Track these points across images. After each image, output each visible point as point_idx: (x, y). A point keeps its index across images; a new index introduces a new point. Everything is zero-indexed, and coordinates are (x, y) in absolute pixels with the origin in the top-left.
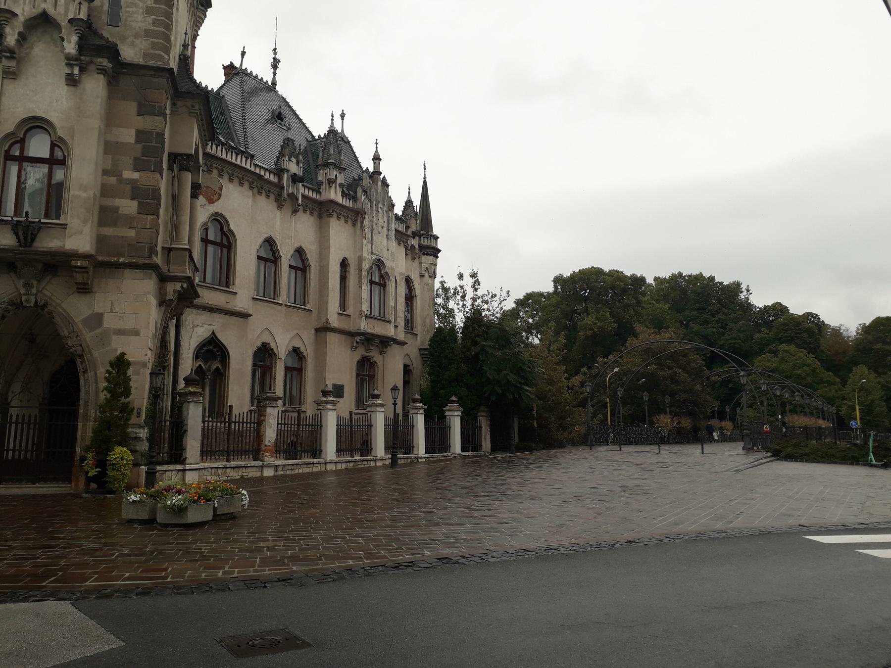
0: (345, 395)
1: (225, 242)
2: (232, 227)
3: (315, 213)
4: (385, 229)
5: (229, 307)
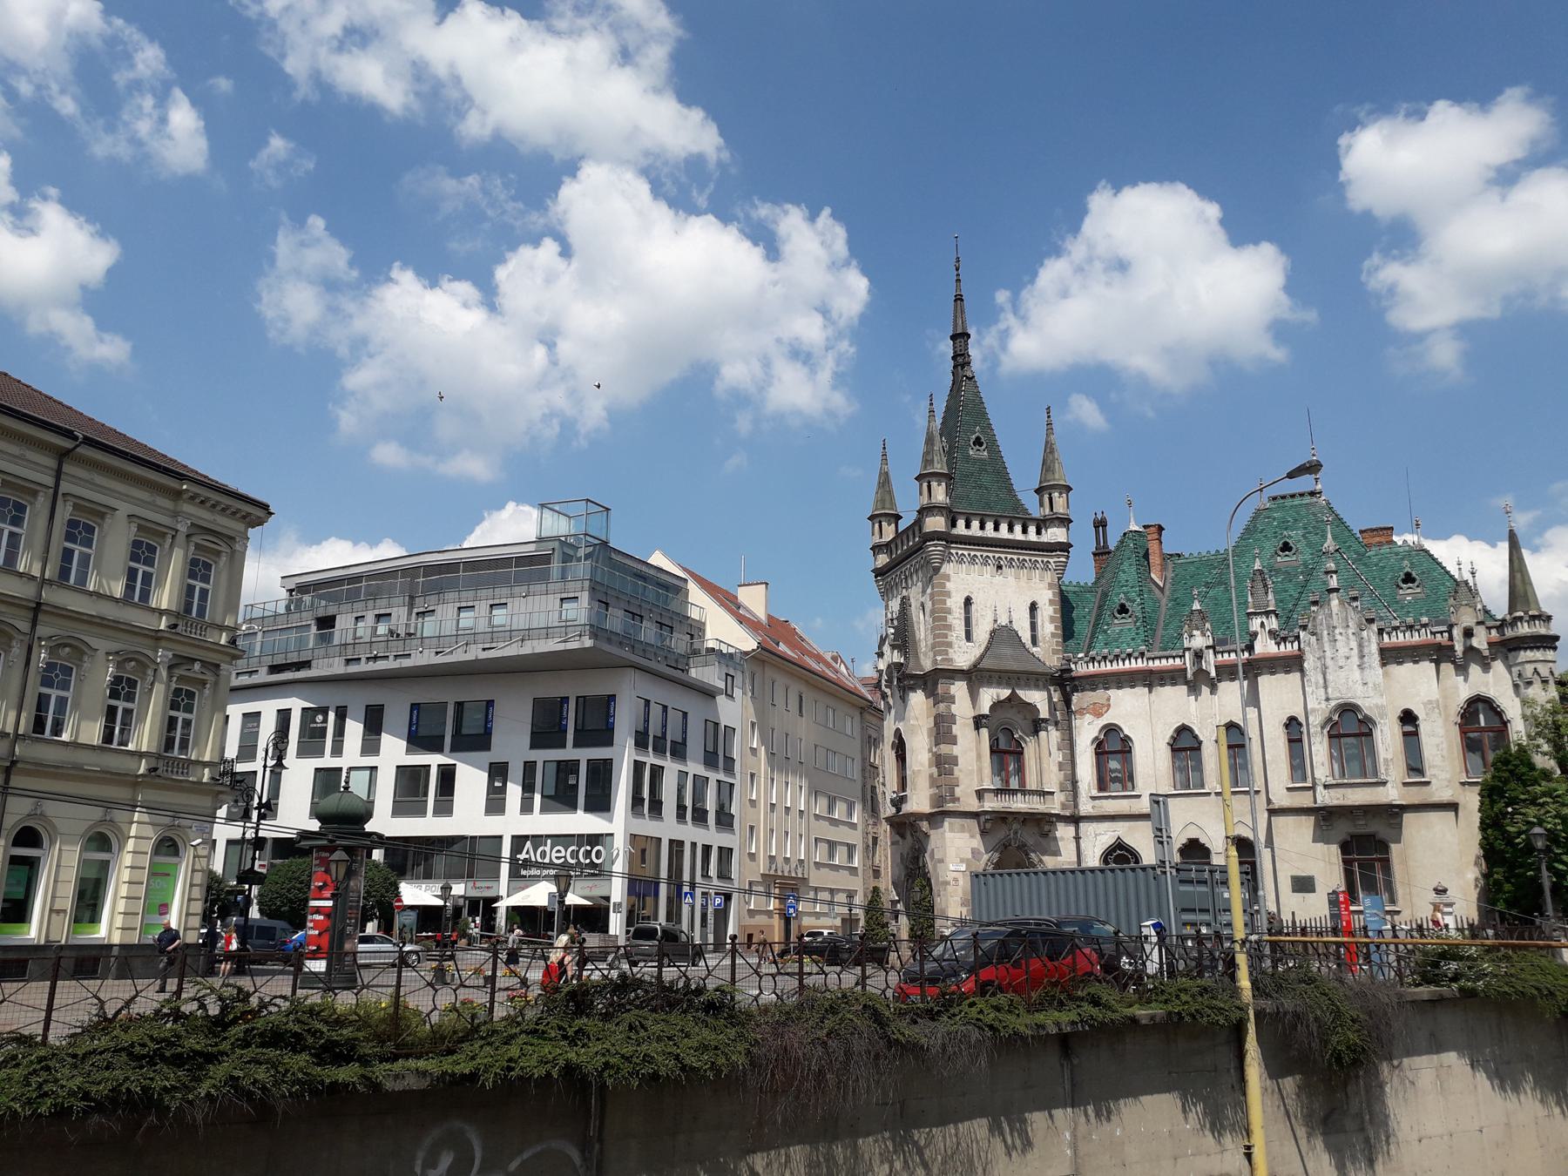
0: (1317, 888)
4: (1355, 660)
5: (1135, 811)
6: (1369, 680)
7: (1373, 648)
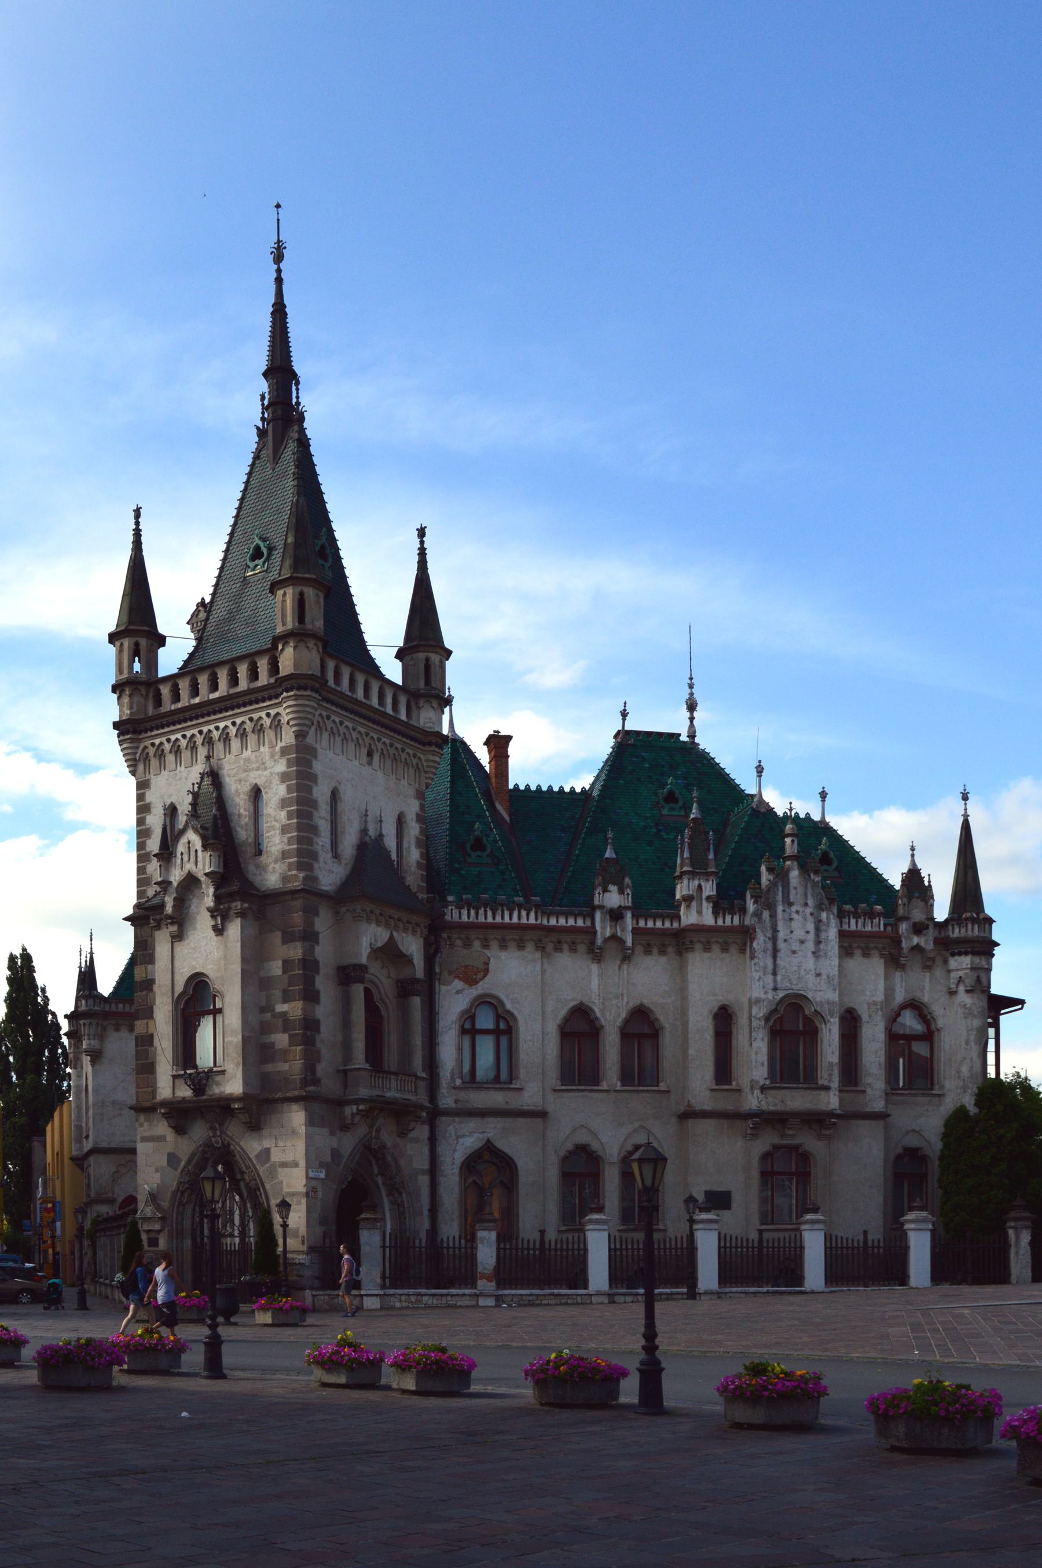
1: (502, 1026)
2: (509, 1006)
3: (670, 950)
4: (810, 945)
6: (824, 972)
7: (832, 933)
